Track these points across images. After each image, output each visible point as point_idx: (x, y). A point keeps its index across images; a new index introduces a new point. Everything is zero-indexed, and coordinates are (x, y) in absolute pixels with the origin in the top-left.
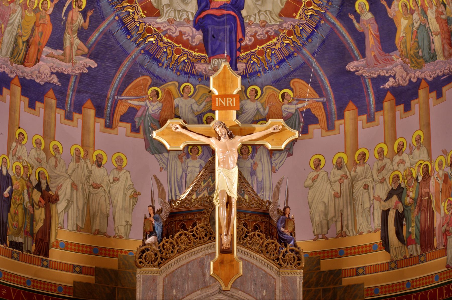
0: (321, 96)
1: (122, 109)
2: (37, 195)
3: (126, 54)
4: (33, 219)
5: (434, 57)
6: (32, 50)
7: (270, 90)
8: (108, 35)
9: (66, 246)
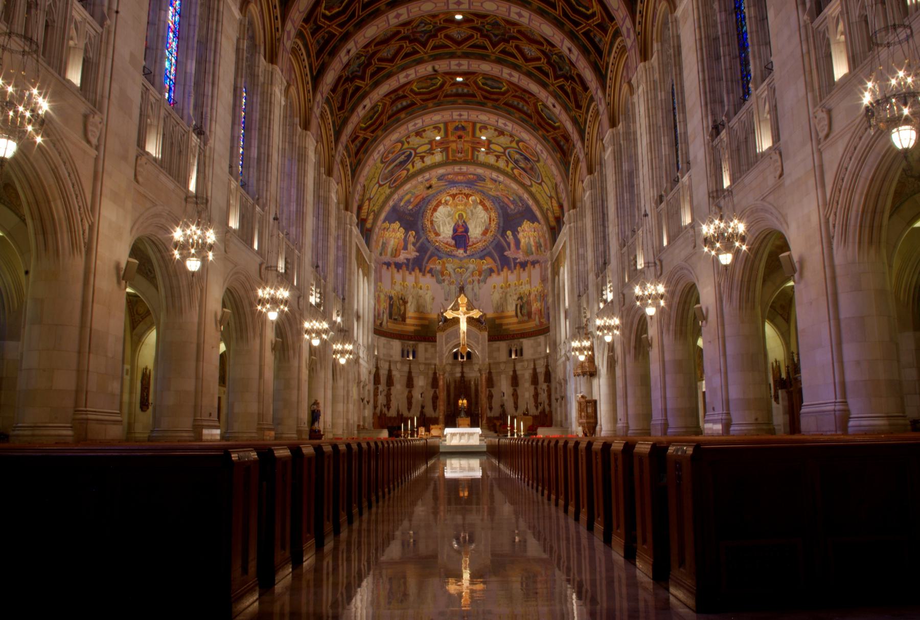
0: (495, 262)
1: (428, 269)
2: (401, 302)
3: (428, 249)
4: (400, 310)
5: (532, 254)
6: (398, 252)
7: (478, 260)
8: (423, 244)
9: (411, 318)
